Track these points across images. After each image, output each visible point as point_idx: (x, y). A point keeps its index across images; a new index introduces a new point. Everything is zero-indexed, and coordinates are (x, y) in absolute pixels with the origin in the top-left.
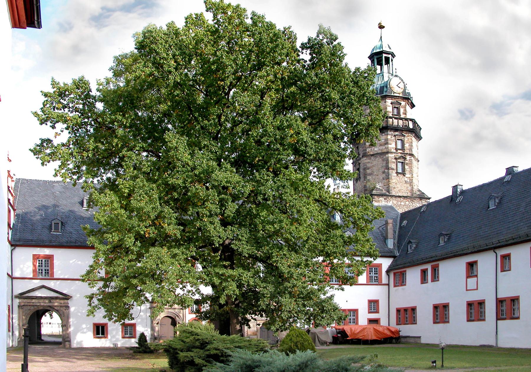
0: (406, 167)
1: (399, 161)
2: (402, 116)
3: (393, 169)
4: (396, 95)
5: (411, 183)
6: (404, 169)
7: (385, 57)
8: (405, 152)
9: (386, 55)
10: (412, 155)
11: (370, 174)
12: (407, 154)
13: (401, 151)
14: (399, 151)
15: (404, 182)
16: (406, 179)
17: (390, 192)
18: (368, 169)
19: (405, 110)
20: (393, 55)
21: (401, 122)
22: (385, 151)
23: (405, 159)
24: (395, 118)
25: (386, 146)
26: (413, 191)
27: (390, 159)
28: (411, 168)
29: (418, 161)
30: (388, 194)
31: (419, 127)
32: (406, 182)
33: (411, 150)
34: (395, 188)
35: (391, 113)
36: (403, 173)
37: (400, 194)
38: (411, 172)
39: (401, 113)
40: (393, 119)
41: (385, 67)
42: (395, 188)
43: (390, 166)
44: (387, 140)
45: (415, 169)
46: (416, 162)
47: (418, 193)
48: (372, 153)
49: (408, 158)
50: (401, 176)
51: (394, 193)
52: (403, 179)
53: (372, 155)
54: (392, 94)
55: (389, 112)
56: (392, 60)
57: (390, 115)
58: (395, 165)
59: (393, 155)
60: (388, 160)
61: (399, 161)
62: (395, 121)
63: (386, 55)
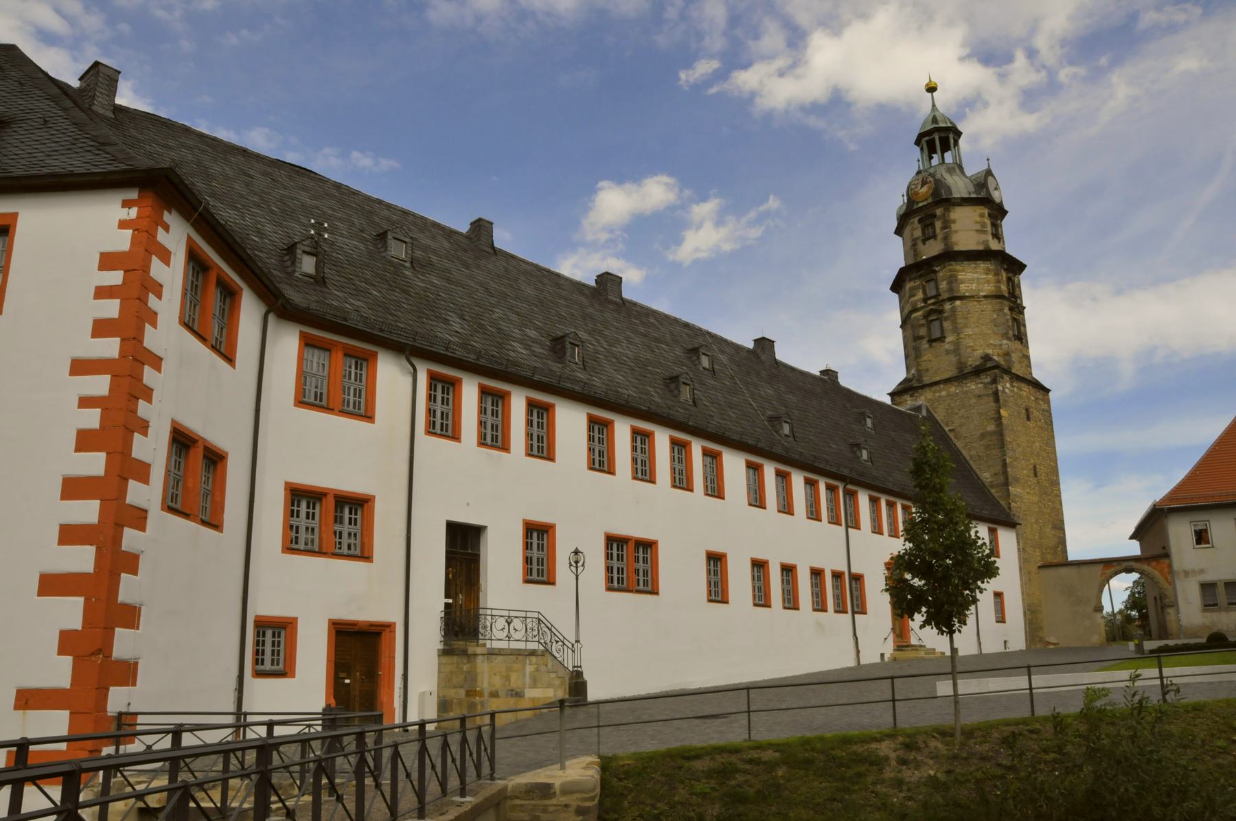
1: (931, 318)
4: (921, 205)
7: (927, 141)
8: (941, 298)
9: (927, 138)
12: (943, 300)
15: (944, 353)
16: (947, 346)
23: (941, 312)
28: (954, 322)
33: (951, 289)
37: (938, 379)
38: (956, 330)
49: (947, 306)
54: (915, 207)
61: (931, 318)
63: (927, 138)
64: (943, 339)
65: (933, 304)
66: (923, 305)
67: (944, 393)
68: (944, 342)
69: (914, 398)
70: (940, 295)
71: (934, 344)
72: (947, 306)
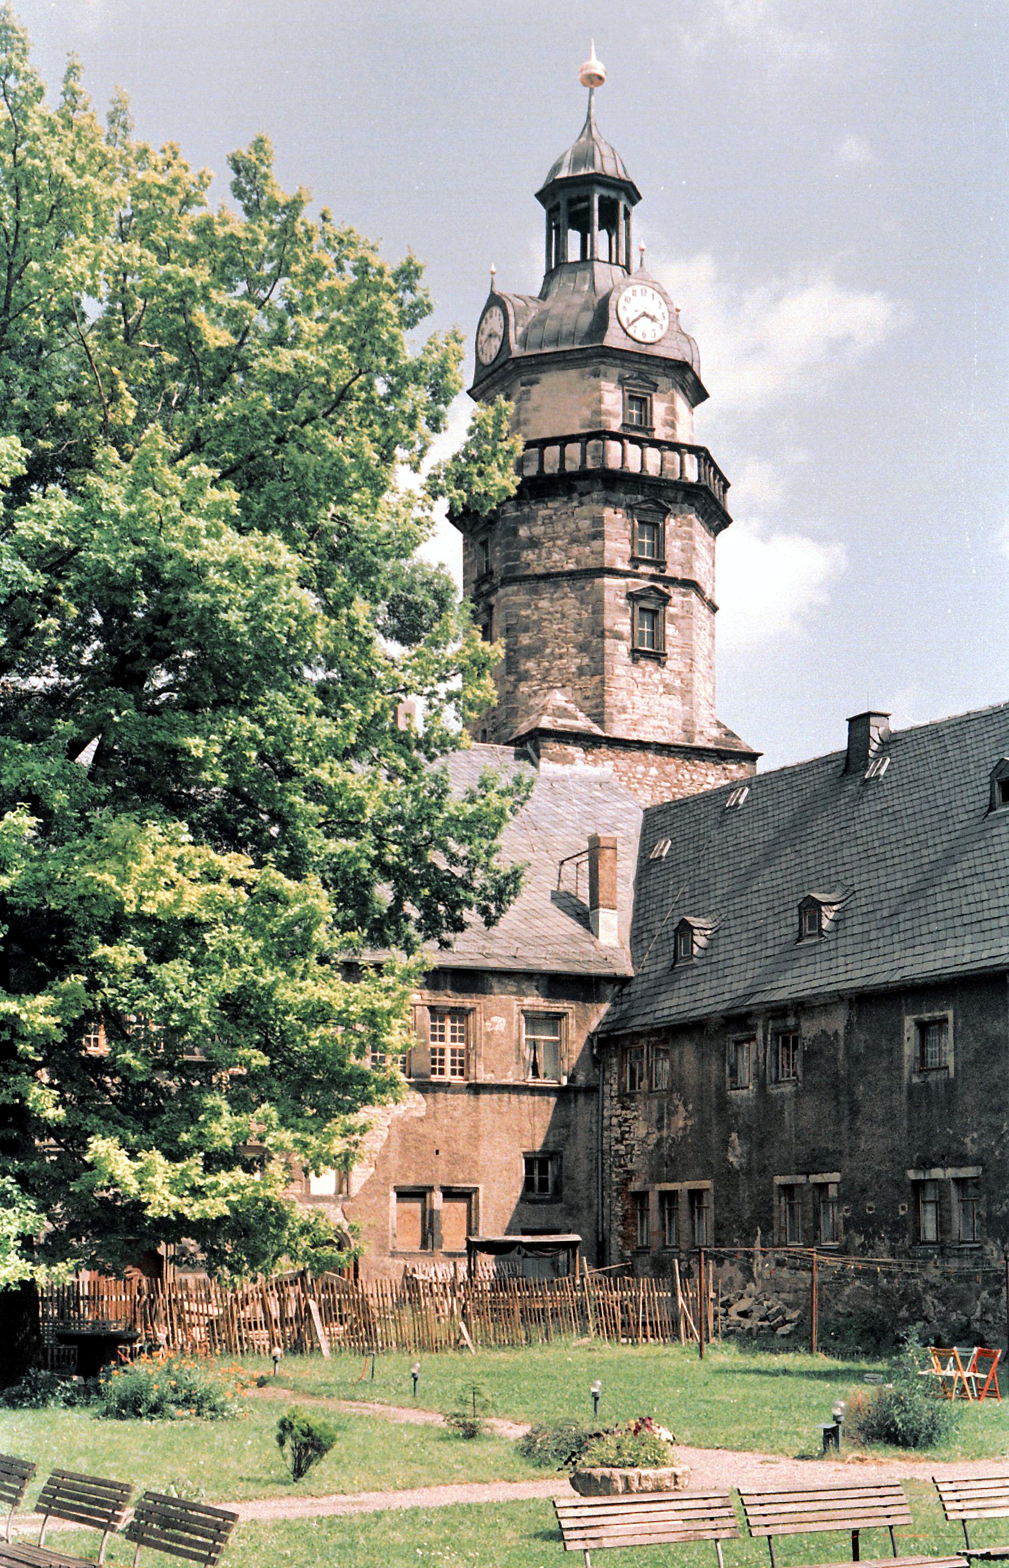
0: (670, 630)
2: (660, 433)
3: (618, 636)
5: (686, 692)
6: (657, 636)
7: (601, 199)
10: (691, 585)
11: (533, 652)
12: (672, 581)
13: (651, 570)
14: (643, 569)
17: (607, 724)
18: (526, 630)
19: (672, 411)
20: (633, 195)
21: (653, 455)
22: (592, 563)
23: (665, 599)
24: (634, 441)
25: (596, 544)
26: (693, 724)
27: (608, 596)
28: (686, 633)
29: (714, 609)
30: (597, 730)
31: (722, 478)
32: (669, 689)
33: (688, 565)
34: (624, 710)
35: (616, 416)
36: (658, 657)
39: (657, 423)
40: (626, 441)
41: (601, 237)
42: (624, 710)
43: (608, 623)
44: (598, 521)
45: (701, 643)
46: (706, 612)
47: (715, 732)
48: (540, 570)
49: (676, 594)
50: (650, 666)
51: (618, 731)
52: (656, 676)
53: (546, 577)
55: (609, 413)
56: (627, 215)
57: (615, 425)
58: (629, 621)
59: (621, 582)
60: (601, 600)
62: (634, 451)
63: (605, 192)
64: (663, 658)
65: (653, 578)
66: (627, 567)
67: (653, 771)
68: (662, 664)
69: (590, 758)
70: (665, 563)
71: (642, 662)
72: (676, 594)
